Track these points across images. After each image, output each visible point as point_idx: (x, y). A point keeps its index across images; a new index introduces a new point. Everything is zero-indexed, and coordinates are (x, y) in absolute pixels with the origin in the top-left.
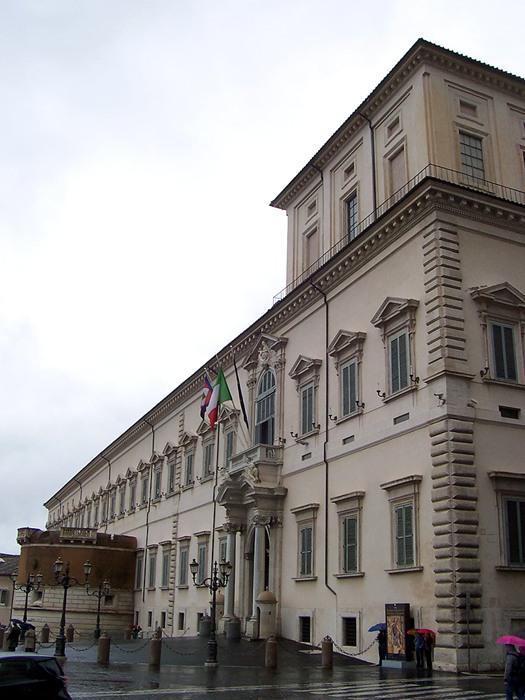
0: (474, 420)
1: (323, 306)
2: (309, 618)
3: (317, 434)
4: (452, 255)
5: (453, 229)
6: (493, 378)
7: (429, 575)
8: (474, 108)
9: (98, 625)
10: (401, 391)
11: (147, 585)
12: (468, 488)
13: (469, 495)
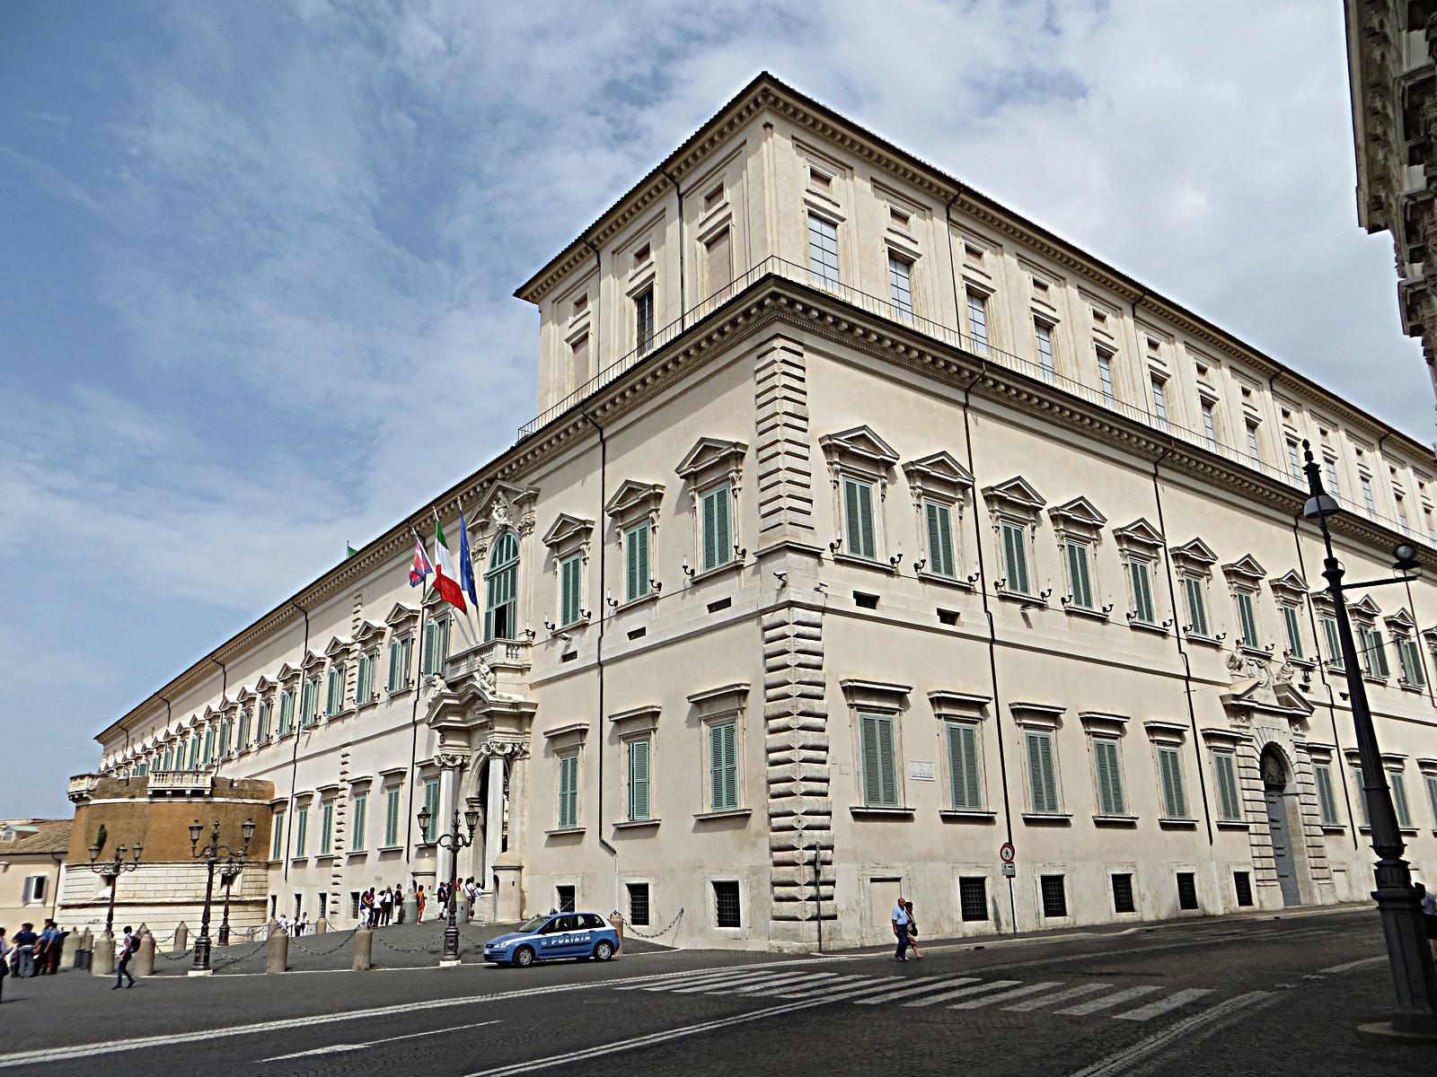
0: (823, 610)
1: (596, 446)
2: (573, 887)
3: (585, 625)
4: (797, 384)
5: (799, 348)
6: (846, 553)
7: (759, 819)
8: (827, 181)
9: (226, 920)
10: (718, 566)
11: (293, 855)
12: (816, 701)
13: (817, 711)
